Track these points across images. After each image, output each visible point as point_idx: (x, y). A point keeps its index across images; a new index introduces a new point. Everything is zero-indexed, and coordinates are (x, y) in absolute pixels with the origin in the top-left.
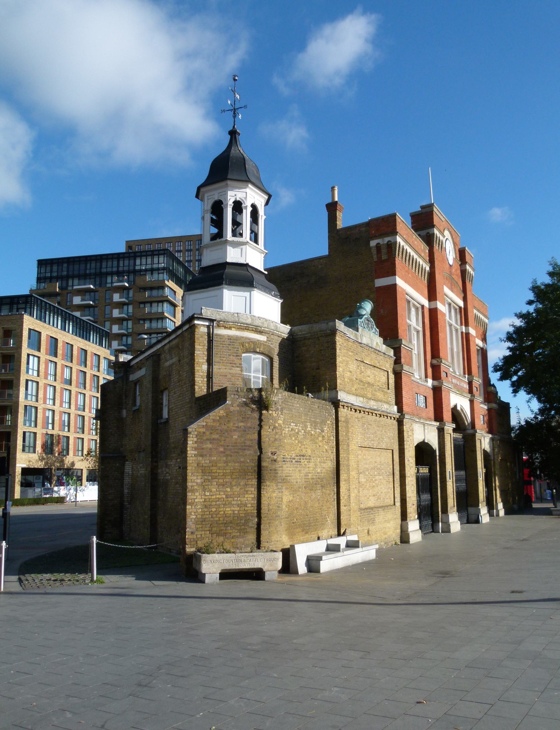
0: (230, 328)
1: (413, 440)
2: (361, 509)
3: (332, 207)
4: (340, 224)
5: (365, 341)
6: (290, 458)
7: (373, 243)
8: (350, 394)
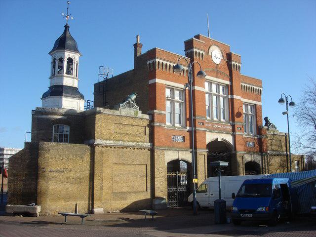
1: (164, 159)
2: (113, 193)
3: (136, 46)
4: (138, 54)
5: (123, 113)
7: (148, 63)
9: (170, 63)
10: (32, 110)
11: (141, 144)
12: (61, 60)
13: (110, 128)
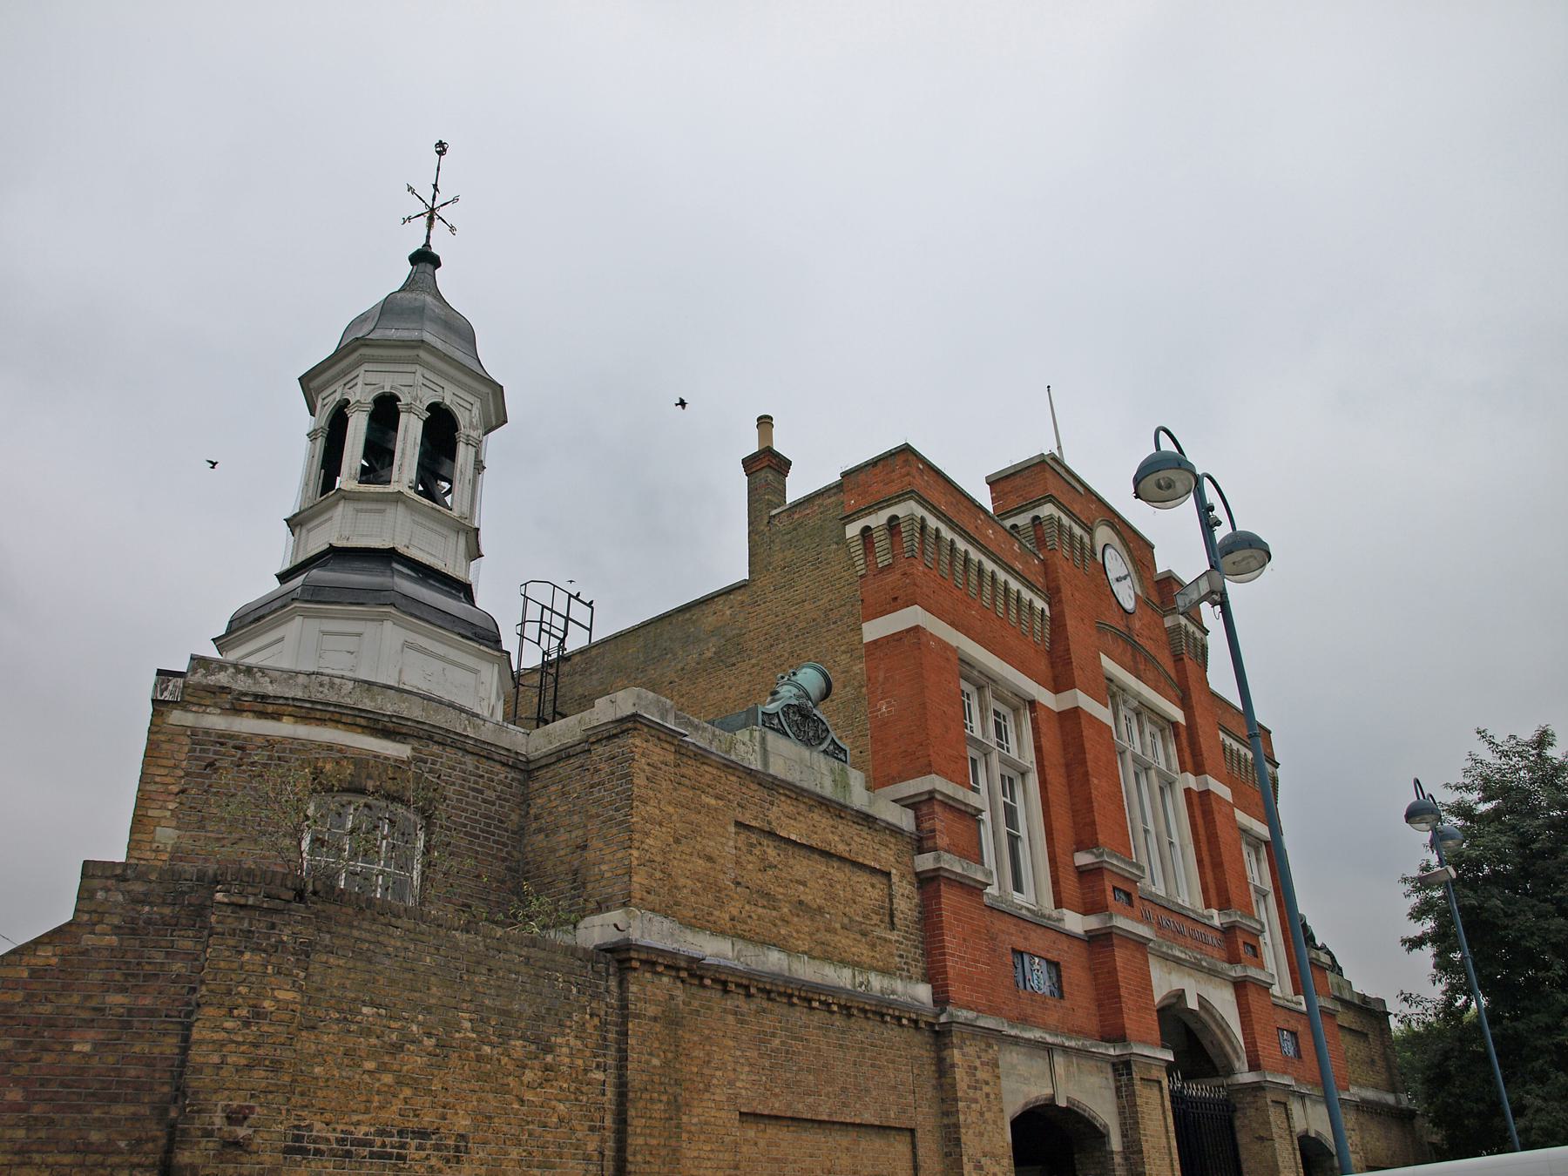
0: (276, 716)
1: (998, 1097)
6: (341, 1141)
7: (853, 530)
8: (703, 928)
9: (971, 550)
10: (160, 672)
11: (877, 983)
12: (385, 412)
13: (711, 846)
